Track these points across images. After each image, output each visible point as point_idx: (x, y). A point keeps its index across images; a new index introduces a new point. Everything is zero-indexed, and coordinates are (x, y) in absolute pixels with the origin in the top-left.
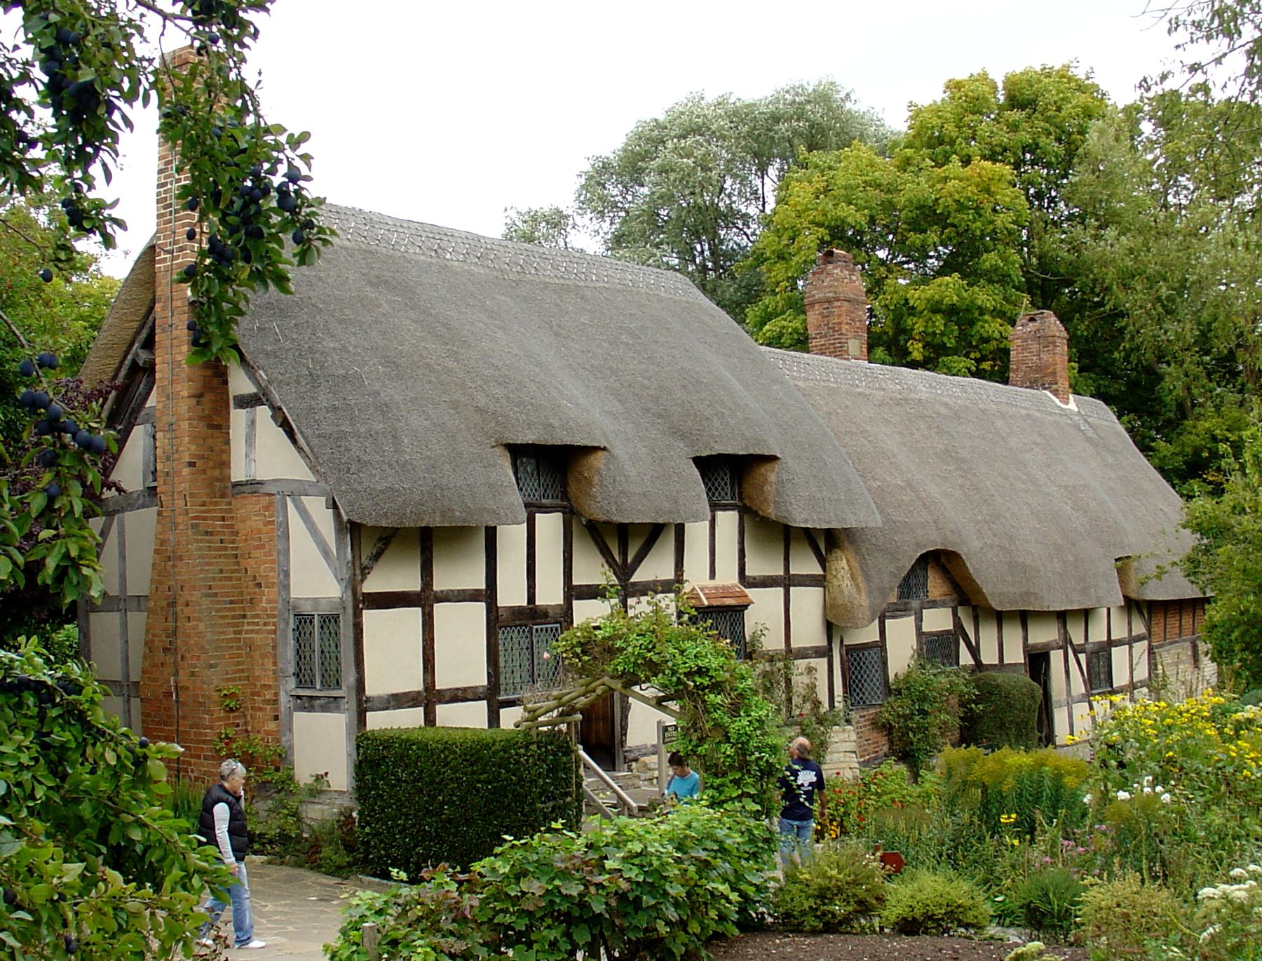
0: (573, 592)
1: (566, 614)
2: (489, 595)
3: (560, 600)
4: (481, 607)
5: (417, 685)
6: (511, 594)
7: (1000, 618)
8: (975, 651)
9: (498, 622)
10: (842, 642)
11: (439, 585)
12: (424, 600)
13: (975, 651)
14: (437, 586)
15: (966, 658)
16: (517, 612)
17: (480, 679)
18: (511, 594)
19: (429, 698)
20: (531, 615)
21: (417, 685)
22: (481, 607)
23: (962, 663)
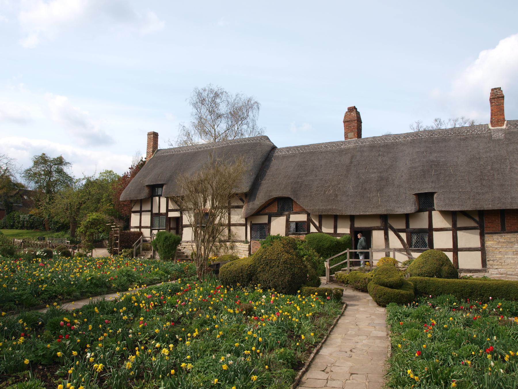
0: (168, 210)
1: (167, 214)
2: (151, 211)
3: (165, 212)
4: (150, 213)
5: (138, 225)
6: (155, 211)
7: (336, 218)
8: (319, 228)
9: (153, 216)
10: (251, 222)
11: (143, 209)
12: (140, 212)
13: (319, 228)
14: (143, 209)
15: (313, 229)
16: (156, 214)
17: (149, 225)
18: (155, 211)
19: (140, 227)
20: (159, 214)
21: (138, 225)
22: (150, 213)
23: (311, 231)
